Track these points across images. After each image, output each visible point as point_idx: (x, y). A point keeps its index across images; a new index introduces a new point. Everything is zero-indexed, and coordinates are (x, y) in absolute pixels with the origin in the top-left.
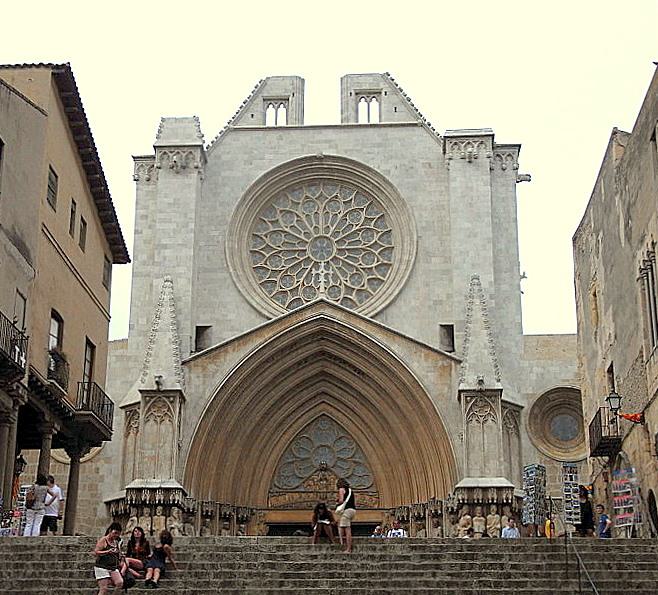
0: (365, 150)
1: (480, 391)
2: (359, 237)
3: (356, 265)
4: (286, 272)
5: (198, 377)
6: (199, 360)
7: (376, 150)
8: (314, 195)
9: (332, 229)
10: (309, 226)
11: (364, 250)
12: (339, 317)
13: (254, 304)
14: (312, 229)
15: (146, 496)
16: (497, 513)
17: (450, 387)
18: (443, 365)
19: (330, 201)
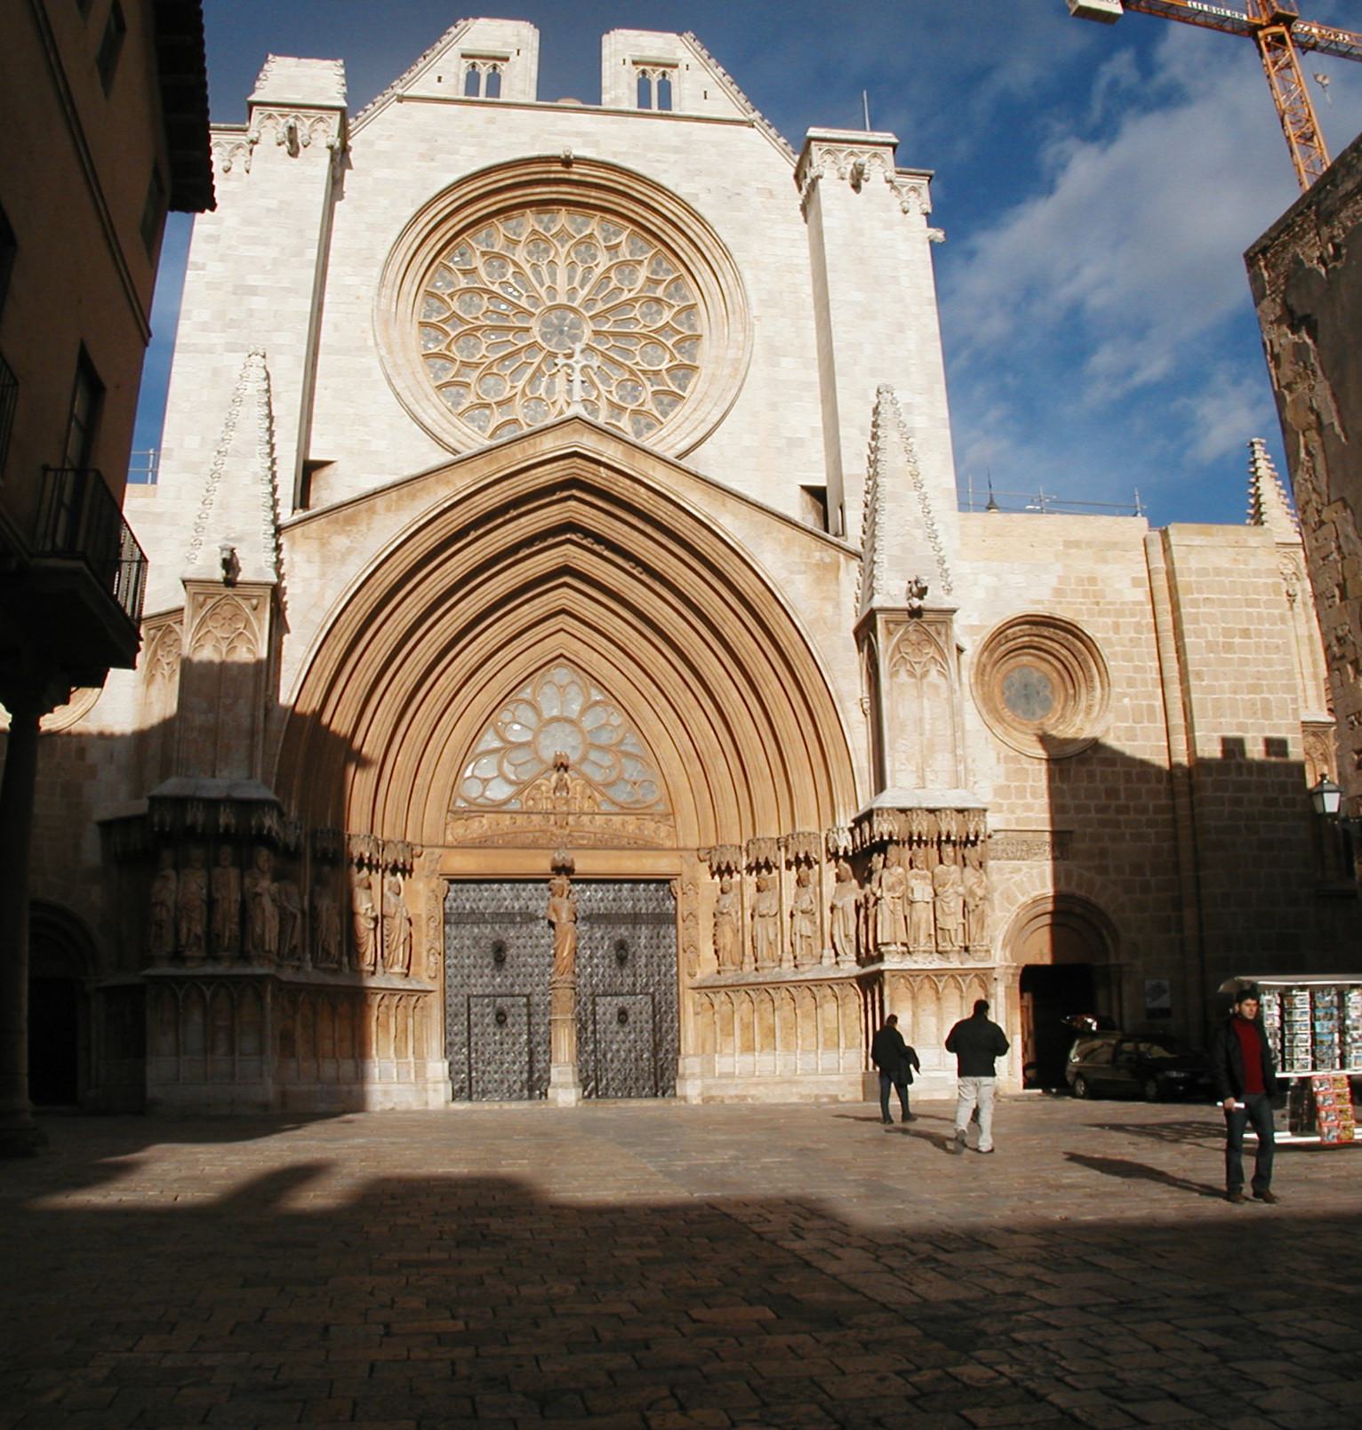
0: (650, 155)
1: (916, 613)
2: (636, 313)
3: (627, 362)
4: (490, 366)
5: (309, 561)
6: (314, 525)
7: (672, 157)
8: (547, 229)
9: (582, 293)
10: (537, 286)
11: (644, 336)
12: (611, 452)
13: (428, 422)
14: (543, 291)
15: (196, 817)
16: (955, 863)
17: (838, 605)
18: (822, 559)
19: (579, 243)
